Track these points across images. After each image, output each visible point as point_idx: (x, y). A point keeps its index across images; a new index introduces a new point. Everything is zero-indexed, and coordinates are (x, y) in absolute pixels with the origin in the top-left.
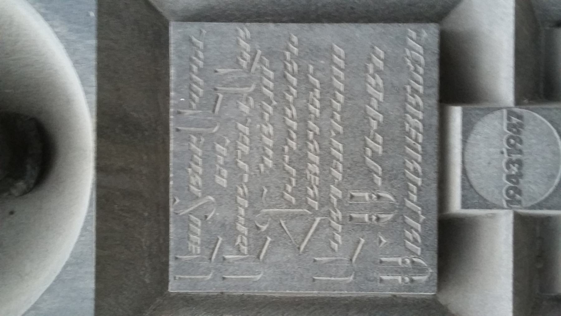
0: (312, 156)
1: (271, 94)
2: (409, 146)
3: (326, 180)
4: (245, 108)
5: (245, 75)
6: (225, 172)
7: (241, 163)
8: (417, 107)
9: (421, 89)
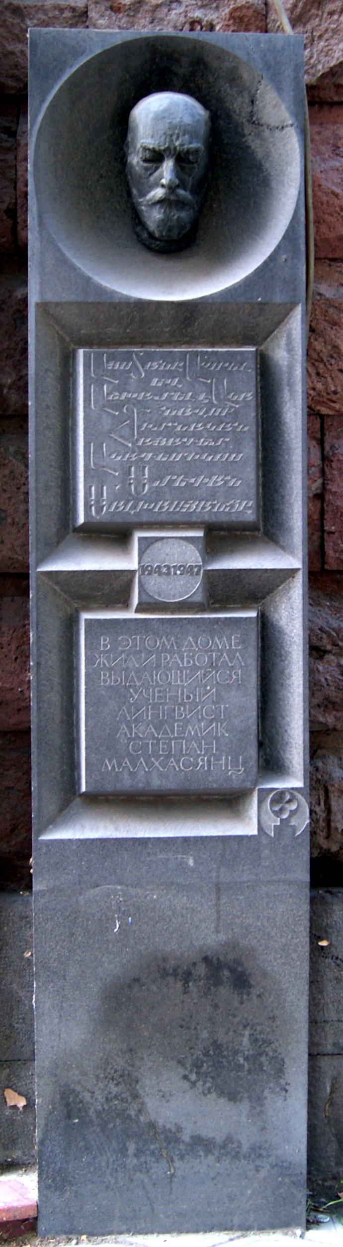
2: (178, 504)
3: (156, 450)
4: (202, 397)
5: (222, 397)
6: (160, 384)
7: (166, 395)
8: (203, 508)
9: (215, 510)
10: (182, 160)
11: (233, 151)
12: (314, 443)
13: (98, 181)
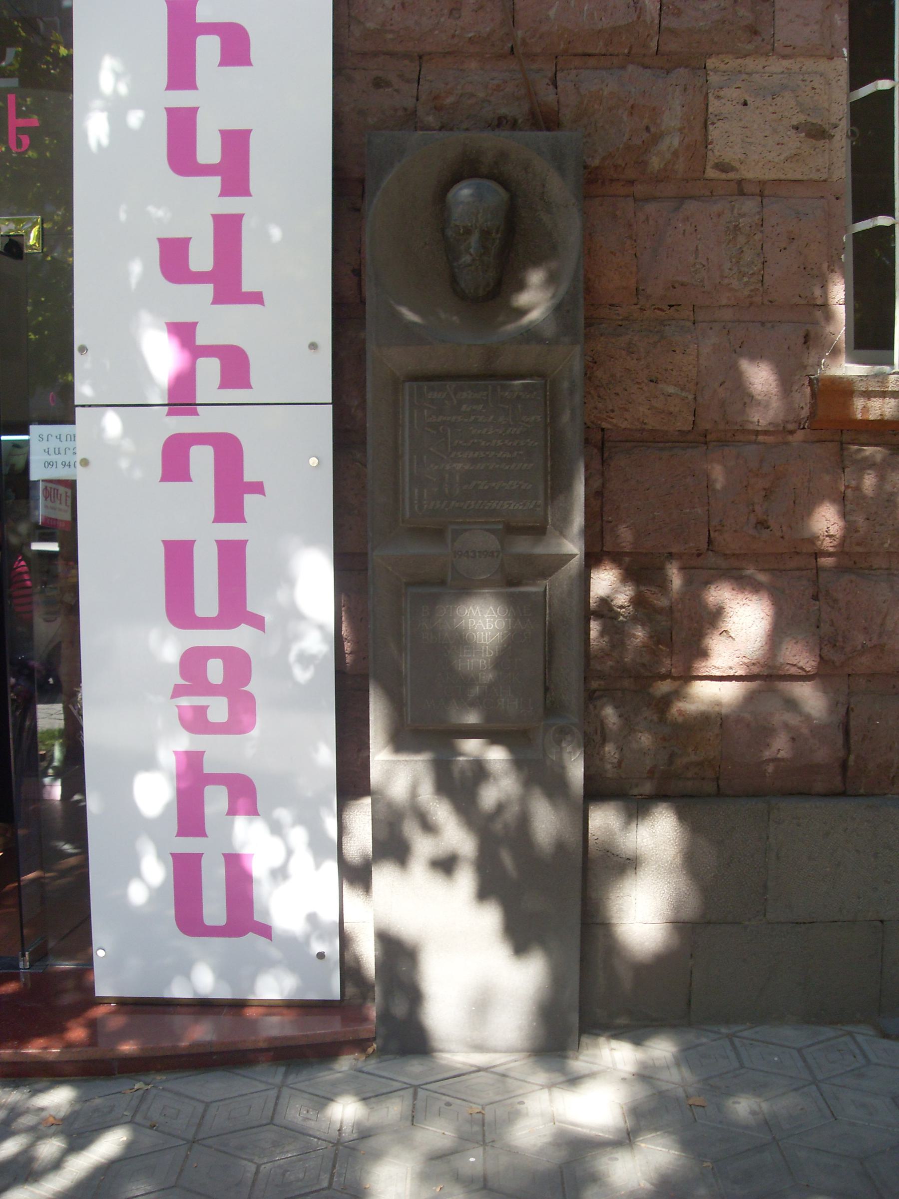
0: (477, 453)
1: (508, 432)
6: (469, 409)
7: (473, 418)
8: (502, 506)
9: (512, 508)
10: (485, 234)
12: (595, 451)
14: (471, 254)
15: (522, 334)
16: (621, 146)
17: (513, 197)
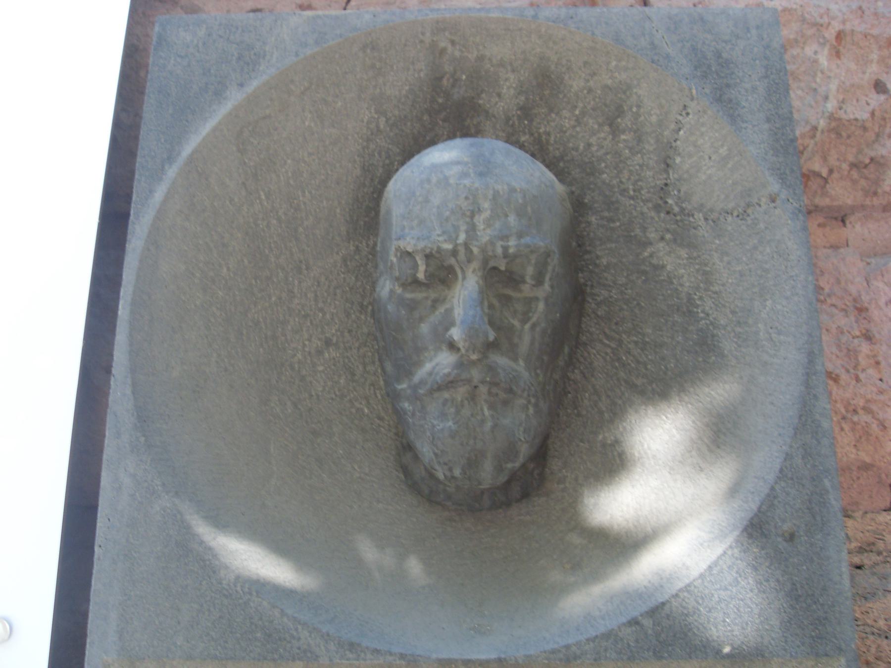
10: (501, 279)
11: (622, 280)
13: (320, 352)
14: (452, 346)
15: (634, 622)
16: (822, 123)
17: (579, 207)
